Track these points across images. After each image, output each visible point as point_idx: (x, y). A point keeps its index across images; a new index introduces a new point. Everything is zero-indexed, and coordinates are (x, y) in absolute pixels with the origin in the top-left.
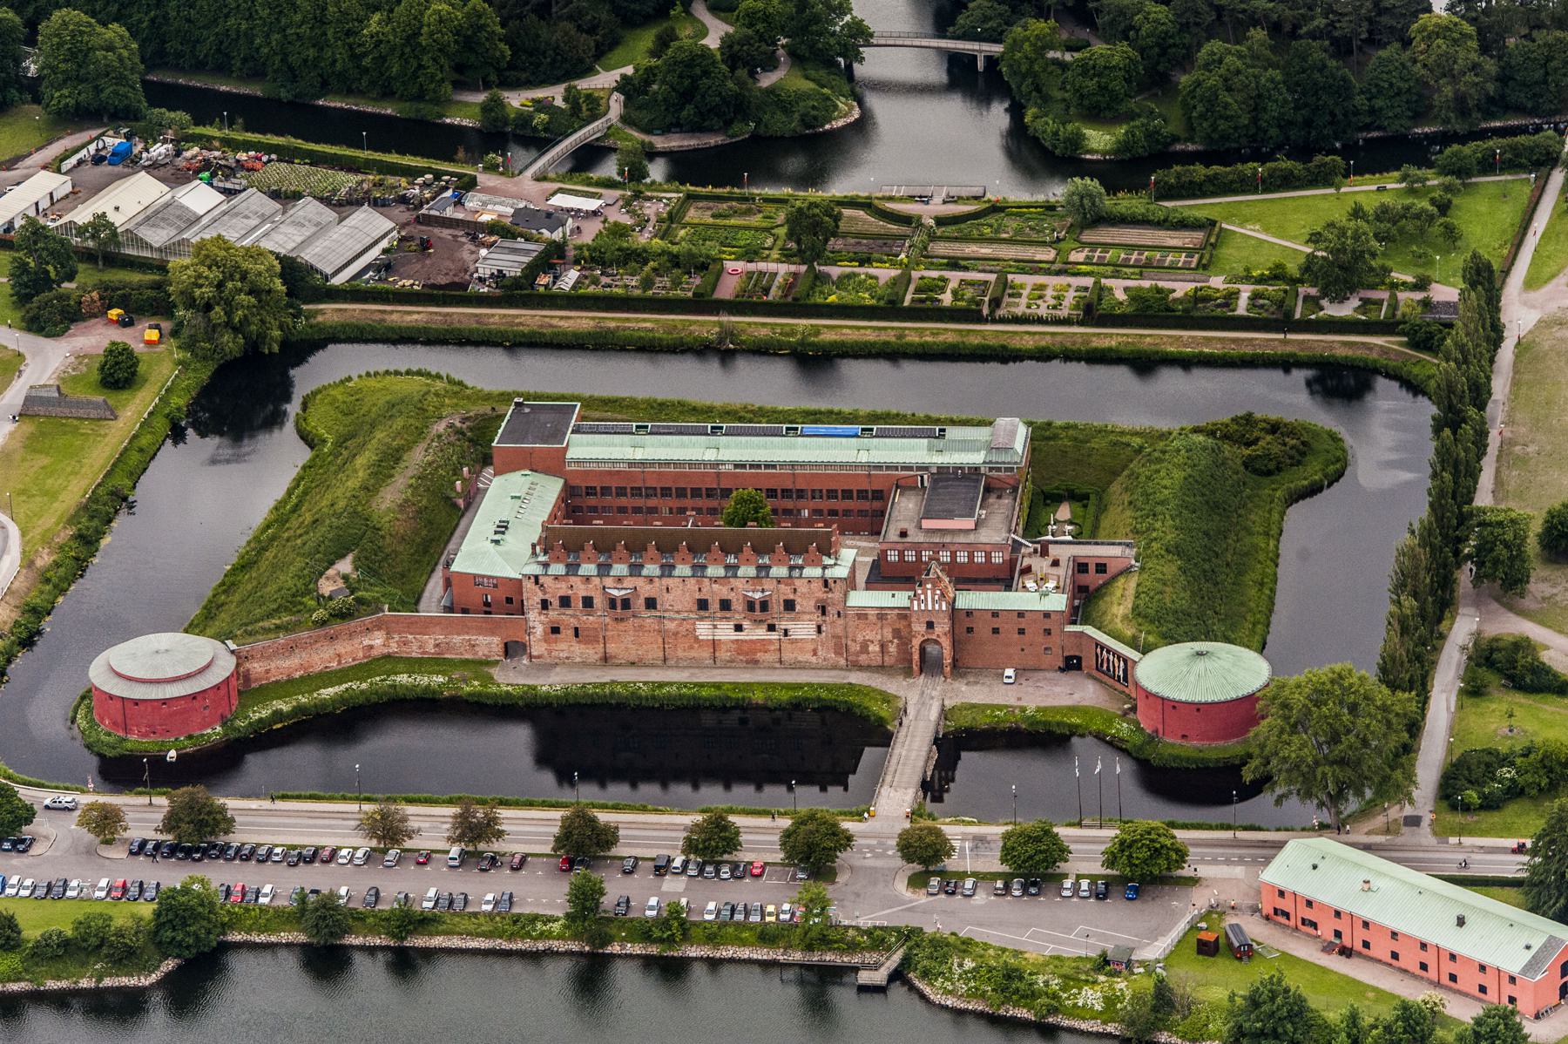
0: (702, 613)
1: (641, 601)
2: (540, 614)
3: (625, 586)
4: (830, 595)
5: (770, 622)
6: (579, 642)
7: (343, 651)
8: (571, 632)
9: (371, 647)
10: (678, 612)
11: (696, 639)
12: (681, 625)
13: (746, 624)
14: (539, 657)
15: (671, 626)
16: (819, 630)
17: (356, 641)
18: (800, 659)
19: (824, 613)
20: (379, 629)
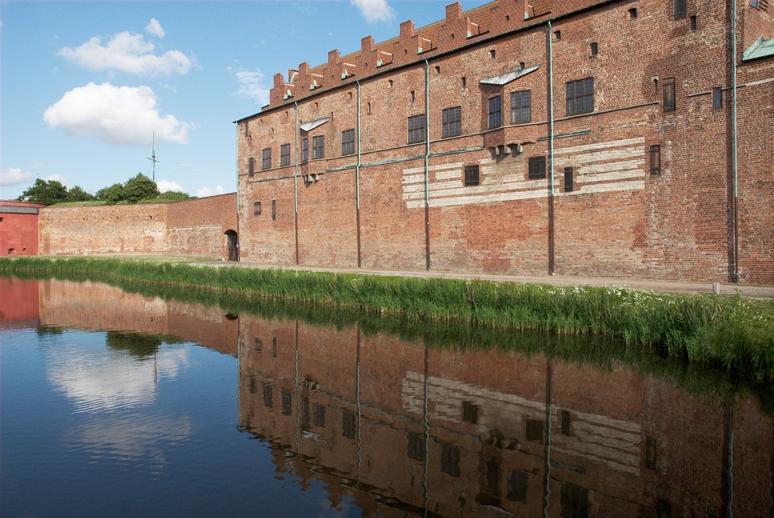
0: (419, 150)
1: (339, 139)
2: (248, 182)
6: (275, 226)
7: (126, 237)
11: (403, 206)
12: (381, 180)
15: (369, 183)
16: (655, 169)
17: (139, 228)
19: (670, 107)
20: (161, 220)
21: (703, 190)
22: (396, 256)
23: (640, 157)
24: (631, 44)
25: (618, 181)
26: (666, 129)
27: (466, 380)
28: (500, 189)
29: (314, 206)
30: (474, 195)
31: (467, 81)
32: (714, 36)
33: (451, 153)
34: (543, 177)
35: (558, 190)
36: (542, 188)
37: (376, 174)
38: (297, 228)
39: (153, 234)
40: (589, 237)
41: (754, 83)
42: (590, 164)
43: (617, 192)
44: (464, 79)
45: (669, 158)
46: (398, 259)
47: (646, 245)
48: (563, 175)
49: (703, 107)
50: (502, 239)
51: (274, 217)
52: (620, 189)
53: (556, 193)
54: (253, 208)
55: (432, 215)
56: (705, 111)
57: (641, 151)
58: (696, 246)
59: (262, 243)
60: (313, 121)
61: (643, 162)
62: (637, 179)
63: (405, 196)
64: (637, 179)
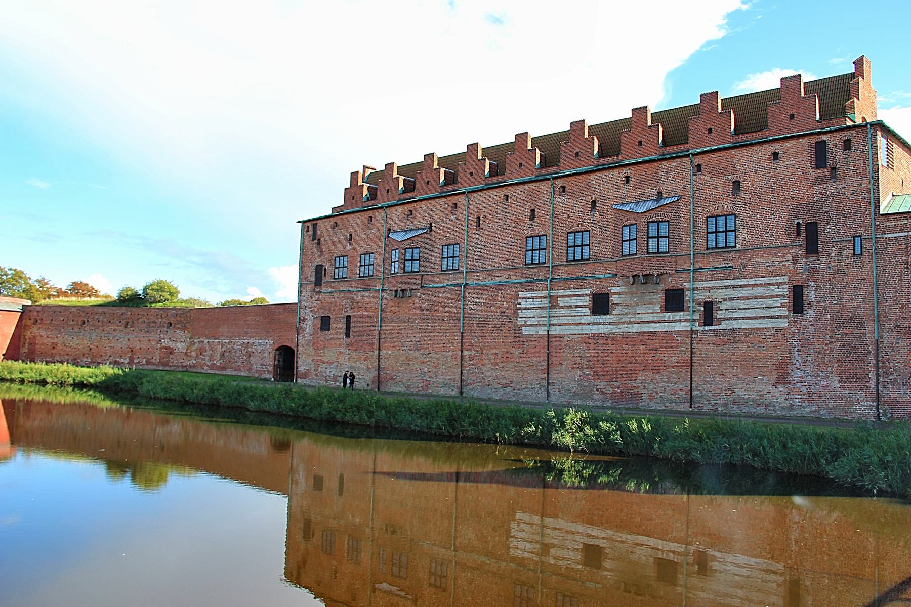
2: (313, 293)
3: (416, 224)
4: (831, 188)
5: (671, 282)
8: (342, 326)
9: (171, 351)
10: (490, 272)
11: (517, 330)
13: (618, 293)
14: (305, 376)
15: (477, 304)
17: (154, 336)
18: (742, 392)
19: (812, 248)
20: (184, 329)
21: (845, 331)
22: (506, 386)
23: (784, 296)
24: (775, 186)
25: (760, 318)
26: (809, 270)
27: (590, 522)
28: (632, 320)
29: (403, 326)
30: (604, 324)
31: (598, 205)
32: (853, 188)
33: (577, 279)
34: (681, 310)
35: (697, 324)
36: (680, 321)
37: (485, 295)
38: (379, 349)
39: (171, 345)
40: (730, 373)
41: (889, 236)
42: (731, 299)
43: (762, 329)
44: (594, 202)
45: (812, 298)
46: (509, 389)
47: (789, 383)
48: (703, 309)
49: (845, 253)
50: (634, 372)
51: (348, 335)
52: (762, 326)
53: (697, 327)
54: (319, 323)
55: (554, 343)
56: (847, 257)
57: (784, 290)
58: (838, 386)
59: (330, 363)
60: (406, 231)
61: (786, 301)
62: (780, 317)
63: (521, 321)
64: (780, 317)
